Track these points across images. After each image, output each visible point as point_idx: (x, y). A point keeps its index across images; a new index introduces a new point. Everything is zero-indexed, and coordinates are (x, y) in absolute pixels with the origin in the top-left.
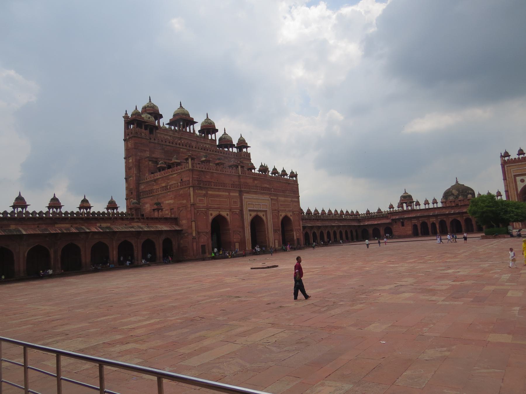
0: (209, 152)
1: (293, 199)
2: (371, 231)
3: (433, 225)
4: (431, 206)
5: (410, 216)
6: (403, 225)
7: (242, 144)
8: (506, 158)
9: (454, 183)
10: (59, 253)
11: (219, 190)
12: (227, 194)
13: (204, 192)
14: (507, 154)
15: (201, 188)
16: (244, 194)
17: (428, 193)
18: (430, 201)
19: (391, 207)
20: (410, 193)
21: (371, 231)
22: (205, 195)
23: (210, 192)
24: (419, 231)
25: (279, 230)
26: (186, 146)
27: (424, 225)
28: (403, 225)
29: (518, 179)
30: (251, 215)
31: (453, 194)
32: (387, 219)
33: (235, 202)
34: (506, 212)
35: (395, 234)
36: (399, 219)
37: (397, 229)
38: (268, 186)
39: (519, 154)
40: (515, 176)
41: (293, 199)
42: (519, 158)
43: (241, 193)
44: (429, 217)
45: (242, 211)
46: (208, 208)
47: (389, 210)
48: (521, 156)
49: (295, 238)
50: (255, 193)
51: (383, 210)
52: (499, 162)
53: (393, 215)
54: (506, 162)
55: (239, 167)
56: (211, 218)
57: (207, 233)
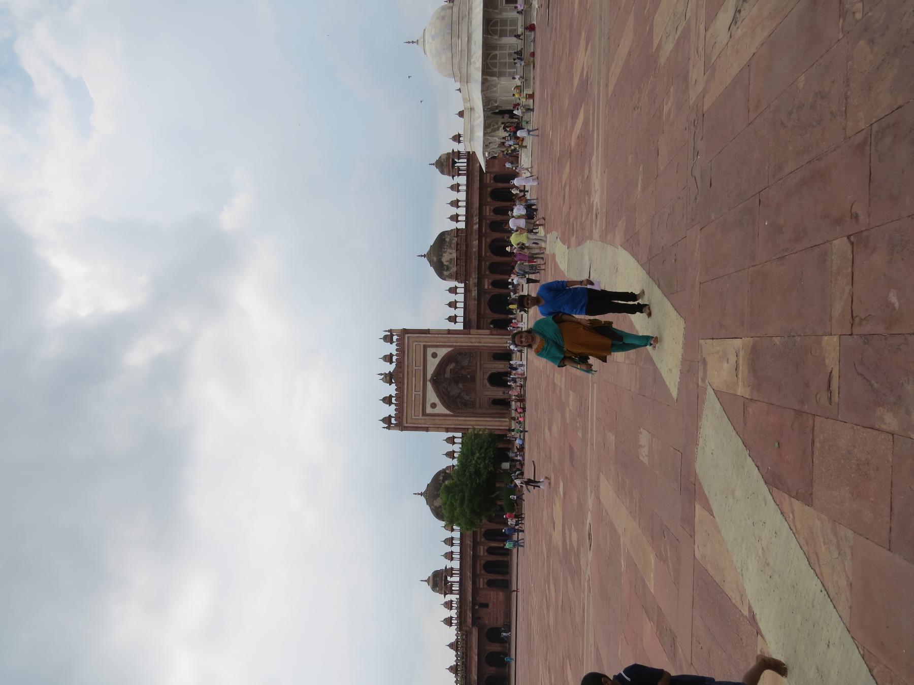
2: (491, 670)
3: (490, 551)
4: (456, 549)
5: (470, 589)
6: (486, 606)
8: (393, 421)
9: (423, 500)
14: (387, 420)
17: (433, 542)
18: (448, 549)
19: (448, 622)
20: (430, 574)
21: (491, 670)
24: (500, 577)
27: (489, 567)
28: (486, 606)
29: (429, 410)
31: (440, 507)
32: (471, 633)
34: (477, 473)
35: (500, 622)
36: (474, 612)
37: (492, 618)
39: (390, 403)
40: (424, 414)
42: (396, 405)
44: (475, 556)
47: (454, 628)
48: (393, 400)
51: (453, 639)
52: (396, 433)
53: (465, 621)
54: (399, 422)
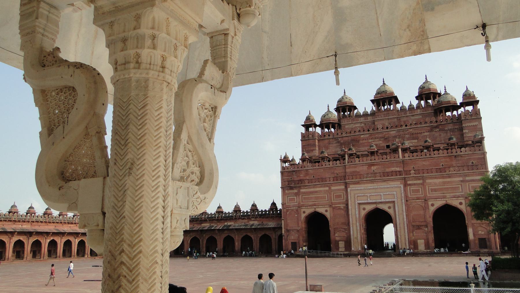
0: (404, 127)
1: (467, 178)
7: (470, 100)
10: (205, 242)
11: (315, 186)
12: (327, 188)
13: (295, 191)
15: (291, 188)
16: (351, 186)
22: (297, 194)
23: (302, 190)
25: (426, 226)
26: (369, 131)
30: (364, 209)
33: (339, 196)
38: (398, 169)
41: (467, 178)
43: (346, 185)
45: (347, 205)
46: (300, 207)
49: (471, 236)
50: (372, 182)
55: (346, 156)
56: (303, 216)
57: (298, 231)
